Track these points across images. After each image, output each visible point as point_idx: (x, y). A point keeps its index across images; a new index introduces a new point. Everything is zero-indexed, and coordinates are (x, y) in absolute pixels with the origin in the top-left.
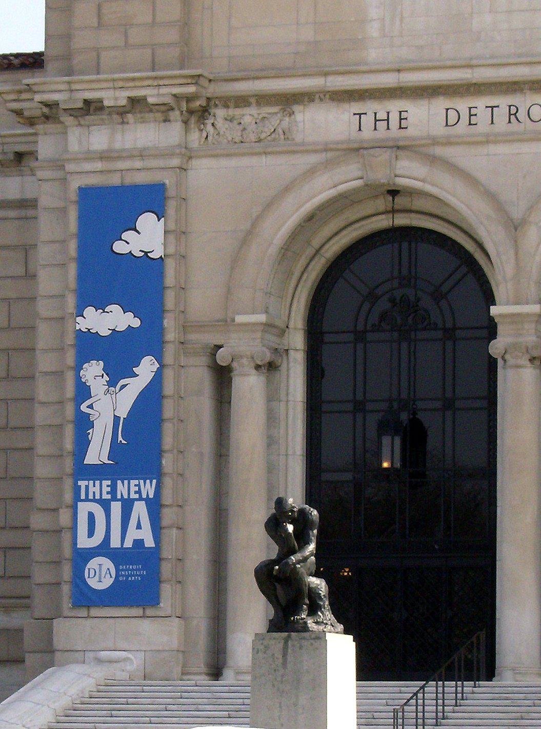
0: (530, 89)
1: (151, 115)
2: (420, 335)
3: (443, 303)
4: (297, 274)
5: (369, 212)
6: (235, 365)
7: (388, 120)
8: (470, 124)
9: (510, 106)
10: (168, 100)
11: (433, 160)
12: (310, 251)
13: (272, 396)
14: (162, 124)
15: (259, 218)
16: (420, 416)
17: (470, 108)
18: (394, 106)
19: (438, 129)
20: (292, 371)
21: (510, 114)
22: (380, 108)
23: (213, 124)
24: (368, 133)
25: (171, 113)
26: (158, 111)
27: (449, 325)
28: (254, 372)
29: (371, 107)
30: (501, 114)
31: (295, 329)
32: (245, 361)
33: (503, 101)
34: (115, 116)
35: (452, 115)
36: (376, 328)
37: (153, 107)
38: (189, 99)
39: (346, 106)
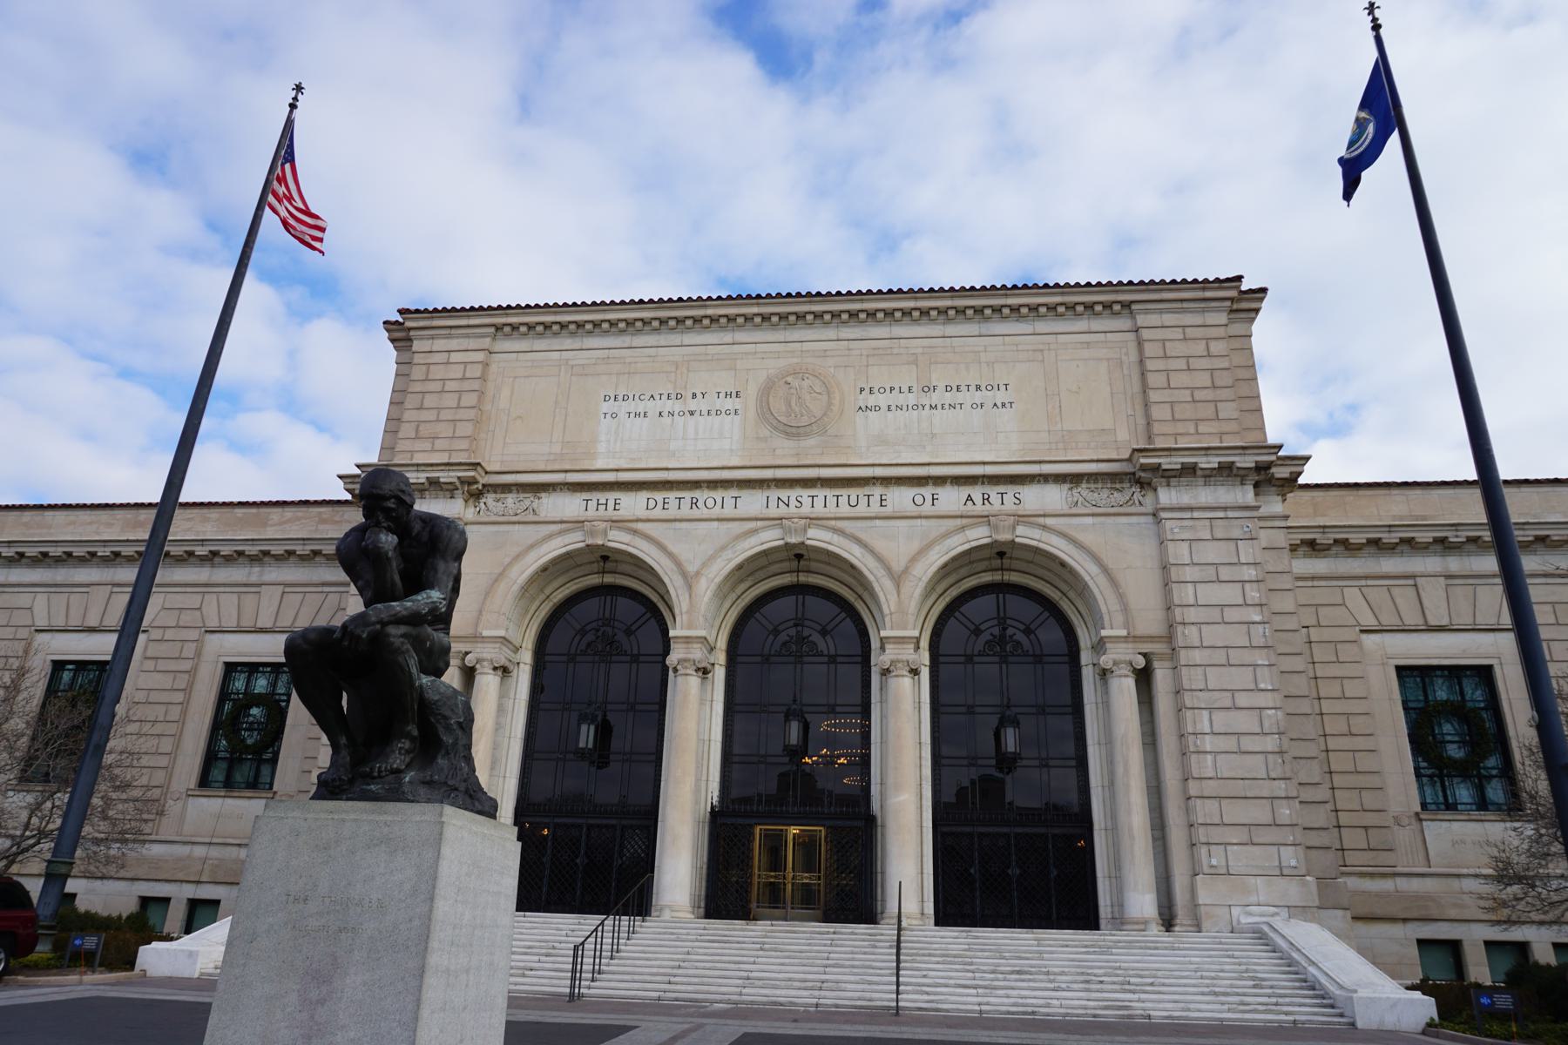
0: (708, 487)
1: (442, 493)
2: (614, 658)
3: (632, 637)
4: (532, 612)
5: (587, 572)
6: (478, 666)
7: (606, 504)
10: (455, 480)
11: (635, 532)
12: (542, 597)
13: (503, 695)
14: (449, 500)
15: (510, 564)
16: (610, 717)
18: (612, 496)
19: (641, 512)
20: (520, 679)
21: (692, 503)
22: (602, 497)
23: (485, 503)
24: (591, 513)
25: (456, 492)
26: (447, 490)
28: (491, 671)
29: (595, 496)
30: (686, 503)
31: (526, 649)
32: (485, 663)
33: (687, 495)
35: (652, 503)
36: (584, 653)
37: (445, 487)
38: (473, 481)
39: (578, 494)
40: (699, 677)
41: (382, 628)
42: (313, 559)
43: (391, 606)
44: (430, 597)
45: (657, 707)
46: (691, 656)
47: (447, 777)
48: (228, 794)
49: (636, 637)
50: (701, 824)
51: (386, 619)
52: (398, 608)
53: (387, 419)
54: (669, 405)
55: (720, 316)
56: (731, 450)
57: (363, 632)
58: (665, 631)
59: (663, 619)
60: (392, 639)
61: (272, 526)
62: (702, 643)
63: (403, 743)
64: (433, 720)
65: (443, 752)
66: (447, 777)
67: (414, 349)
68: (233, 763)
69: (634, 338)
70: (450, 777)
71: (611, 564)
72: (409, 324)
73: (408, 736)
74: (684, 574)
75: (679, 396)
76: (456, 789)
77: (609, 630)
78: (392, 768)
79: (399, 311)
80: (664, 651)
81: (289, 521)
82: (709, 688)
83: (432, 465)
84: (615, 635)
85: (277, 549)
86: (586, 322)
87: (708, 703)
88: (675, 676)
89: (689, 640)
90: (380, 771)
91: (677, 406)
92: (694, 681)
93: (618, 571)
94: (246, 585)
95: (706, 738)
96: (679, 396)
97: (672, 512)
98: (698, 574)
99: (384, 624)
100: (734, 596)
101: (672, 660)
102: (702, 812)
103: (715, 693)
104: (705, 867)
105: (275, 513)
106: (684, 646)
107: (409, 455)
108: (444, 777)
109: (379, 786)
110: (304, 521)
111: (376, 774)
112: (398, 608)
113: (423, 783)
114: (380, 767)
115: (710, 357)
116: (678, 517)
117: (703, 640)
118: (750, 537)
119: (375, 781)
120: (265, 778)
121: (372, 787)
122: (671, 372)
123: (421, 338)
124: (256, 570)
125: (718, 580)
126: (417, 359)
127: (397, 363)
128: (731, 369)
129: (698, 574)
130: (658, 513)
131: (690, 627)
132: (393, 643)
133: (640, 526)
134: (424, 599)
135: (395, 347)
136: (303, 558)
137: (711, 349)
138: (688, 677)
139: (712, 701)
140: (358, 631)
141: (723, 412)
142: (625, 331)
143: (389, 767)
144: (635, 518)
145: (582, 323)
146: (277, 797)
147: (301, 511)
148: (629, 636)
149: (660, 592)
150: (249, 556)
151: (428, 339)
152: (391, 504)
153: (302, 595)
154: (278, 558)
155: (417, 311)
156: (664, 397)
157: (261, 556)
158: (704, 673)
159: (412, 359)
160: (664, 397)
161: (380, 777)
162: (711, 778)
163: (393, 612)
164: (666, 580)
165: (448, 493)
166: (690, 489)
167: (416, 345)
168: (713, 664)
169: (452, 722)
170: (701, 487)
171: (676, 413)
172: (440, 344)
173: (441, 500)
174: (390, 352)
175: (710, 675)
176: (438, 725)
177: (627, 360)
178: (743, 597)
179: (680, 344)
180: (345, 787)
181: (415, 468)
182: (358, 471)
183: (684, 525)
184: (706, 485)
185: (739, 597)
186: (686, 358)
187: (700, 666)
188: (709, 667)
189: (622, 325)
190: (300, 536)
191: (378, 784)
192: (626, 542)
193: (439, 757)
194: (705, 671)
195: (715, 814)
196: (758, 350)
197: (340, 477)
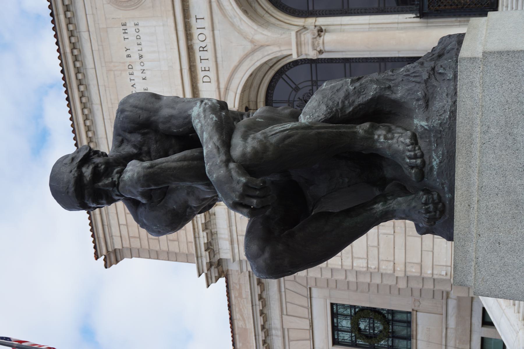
0: (191, 40)
1: (212, 221)
3: (300, 86)
8: (209, 70)
9: (200, 51)
11: (227, 89)
14: (216, 216)
17: (202, 71)
19: (213, 85)
21: (203, 51)
26: (210, 218)
27: (310, 83)
30: (204, 55)
33: (198, 55)
34: (213, 237)
37: (208, 220)
40: (324, 34)
41: (234, 162)
42: (264, 299)
43: (207, 154)
44: (199, 115)
45: (348, 65)
46: (310, 41)
47: (419, 83)
48: (414, 337)
49: (299, 84)
50: (429, 25)
51: (223, 158)
52: (210, 146)
53: (168, 260)
54: (137, 73)
55: (70, 42)
56: (163, 25)
57: (238, 182)
58: (296, 63)
59: (286, 65)
60: (249, 149)
61: (246, 325)
62: (300, 34)
63: (379, 136)
64: (351, 109)
65: (388, 93)
66: (419, 83)
67: (120, 247)
68: (394, 336)
69: (94, 103)
70: (418, 79)
71: (251, 106)
72: (104, 252)
73: (370, 133)
74: (253, 51)
75: (130, 67)
76: (433, 69)
77: (296, 103)
78: (412, 144)
79: (97, 259)
80: (308, 63)
81: (242, 315)
82: (332, 28)
83: (194, 229)
84: (299, 98)
85: (260, 321)
86: (87, 136)
87: (343, 27)
88: (326, 52)
89: (299, 43)
90: (415, 157)
91: (137, 68)
92: (327, 37)
93: (255, 100)
94: (284, 337)
95: (367, 26)
96: (130, 67)
97: (211, 64)
98: (252, 42)
99: (229, 159)
100: (267, 16)
101: (312, 54)
102: (419, 25)
103: (335, 23)
104: (459, 19)
105: (238, 324)
106: (303, 47)
107: (189, 244)
108: (418, 85)
109: (434, 155)
110: (241, 307)
111: (419, 161)
112: (210, 146)
113: (427, 106)
114: (410, 158)
115: (101, 48)
116: (214, 59)
117: (298, 34)
118: (223, 7)
119: (427, 162)
120: (404, 317)
121: (434, 163)
122: (114, 74)
123: (113, 243)
124: (274, 332)
125: (255, 26)
126: (126, 245)
127: (132, 258)
128: (107, 31)
129: (252, 42)
130: (212, 74)
131: (290, 44)
132: (254, 148)
133: (222, 86)
134: (200, 122)
135: (121, 260)
136: (264, 305)
137: (95, 47)
138: (325, 42)
139: (341, 25)
140: (239, 188)
141: (137, 34)
142: (90, 109)
143: (410, 148)
144: (217, 90)
145: (89, 139)
146: (416, 309)
147: (235, 309)
148: (300, 89)
149: (267, 69)
150: (265, 337)
151: (113, 239)
152: (87, 171)
153: (288, 304)
154: (265, 320)
155: (95, 247)
156: (132, 77)
157: (265, 330)
158: (322, 32)
159: (127, 248)
160: (132, 77)
161: (422, 156)
162: (396, 21)
163: (215, 151)
164: (258, 64)
165: (211, 217)
166: (194, 53)
167: (118, 246)
168: (315, 26)
169: (351, 88)
170: (191, 45)
171: (143, 68)
172: (115, 231)
173: (217, 221)
174: (125, 262)
175: (323, 28)
176: (356, 103)
177: (110, 105)
178: (266, 9)
179: (94, 70)
180: (435, 196)
181: (197, 239)
182: (203, 276)
183: (219, 55)
184: (189, 42)
185: (267, 12)
186: (104, 65)
187: (317, 34)
188: (317, 28)
189: (86, 111)
190: (251, 308)
191: (431, 157)
192: (234, 95)
193: (393, 96)
194: (320, 31)
195: (423, 14)
196: (91, 13)
197: (208, 286)
